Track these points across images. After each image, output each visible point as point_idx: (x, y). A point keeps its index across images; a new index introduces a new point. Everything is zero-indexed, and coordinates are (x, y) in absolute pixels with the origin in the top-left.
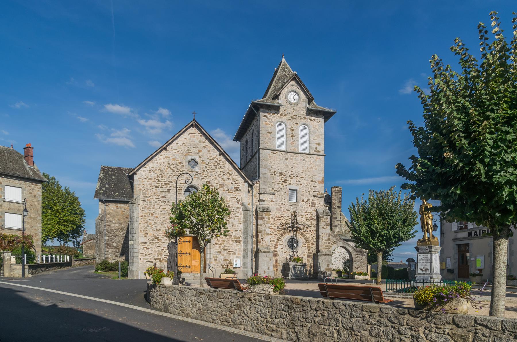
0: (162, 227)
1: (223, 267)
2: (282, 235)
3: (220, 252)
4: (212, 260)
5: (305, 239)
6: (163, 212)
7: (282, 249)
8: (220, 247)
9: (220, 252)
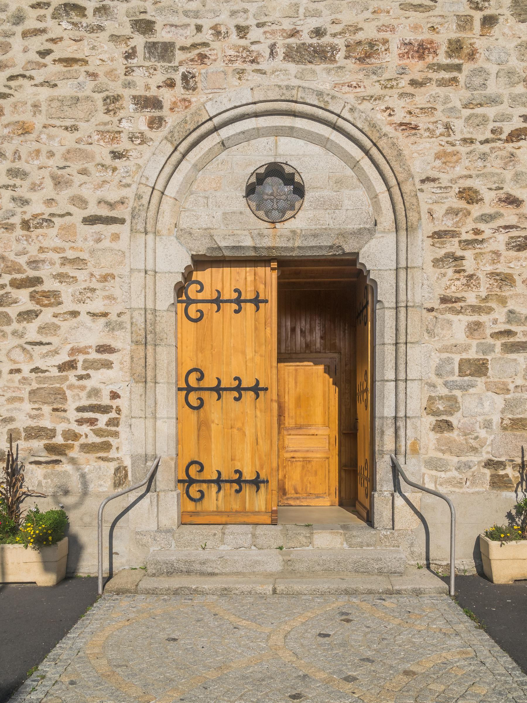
0: (63, 196)
1: (499, 483)
3: (479, 368)
4: (421, 429)
6: (66, 89)
8: (474, 328)
9: (479, 368)
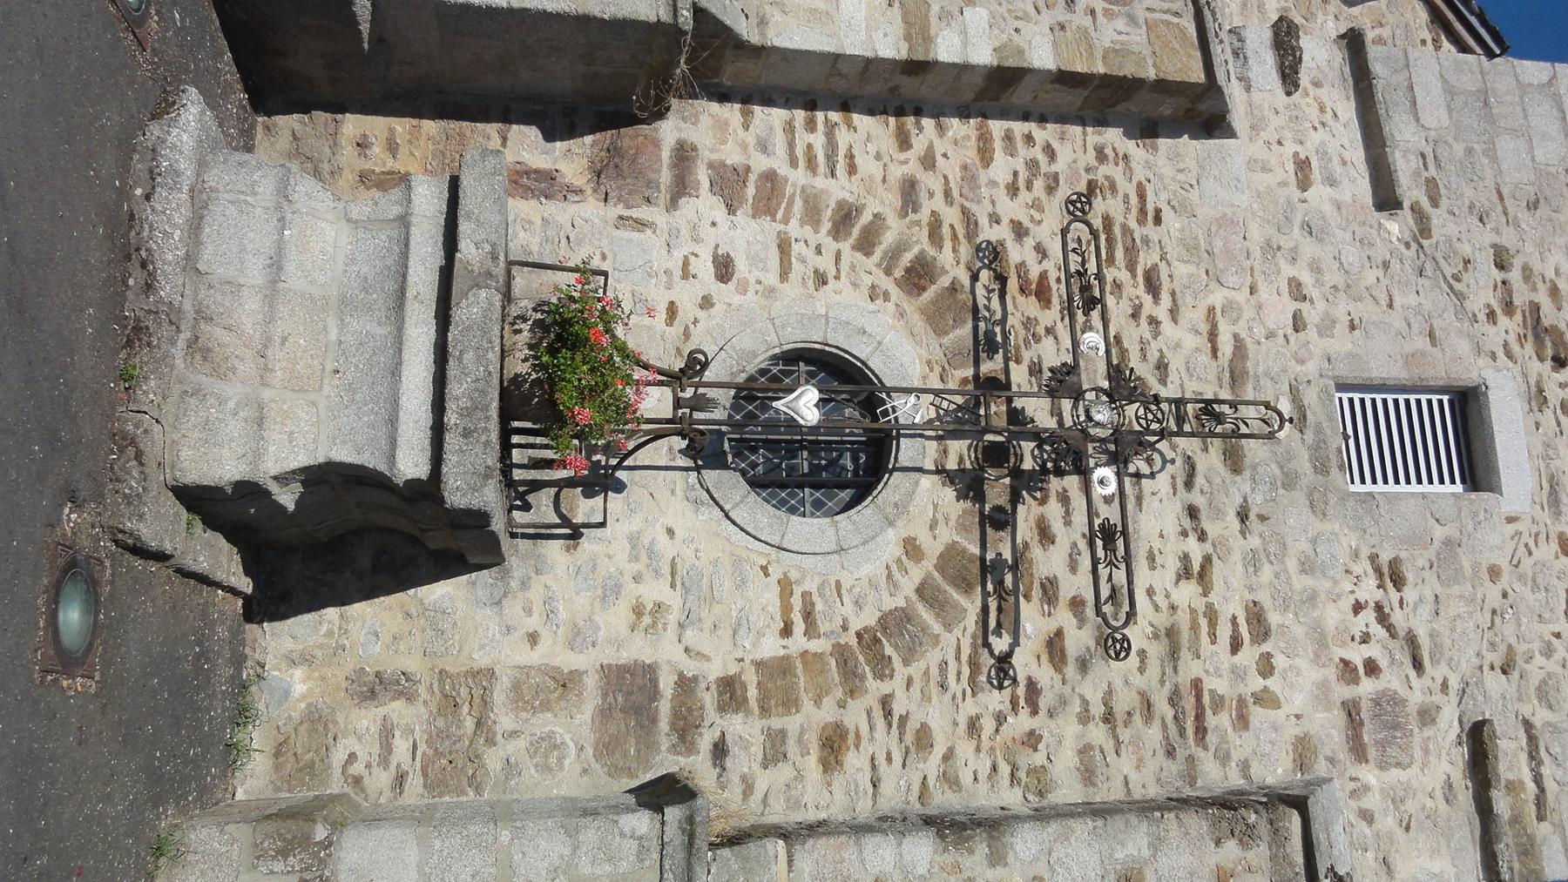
2: (918, 276)
5: (896, 622)
7: (724, 269)
